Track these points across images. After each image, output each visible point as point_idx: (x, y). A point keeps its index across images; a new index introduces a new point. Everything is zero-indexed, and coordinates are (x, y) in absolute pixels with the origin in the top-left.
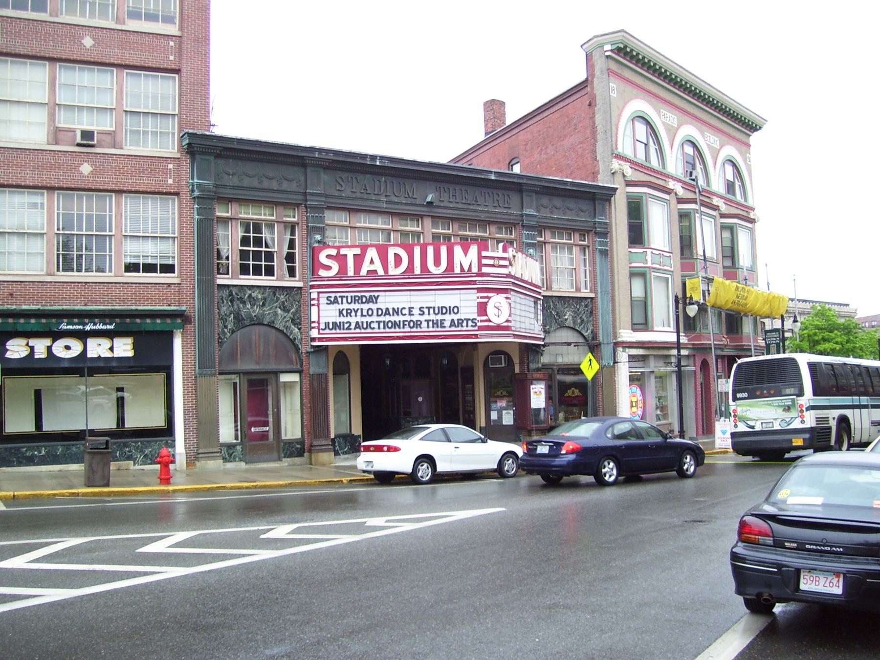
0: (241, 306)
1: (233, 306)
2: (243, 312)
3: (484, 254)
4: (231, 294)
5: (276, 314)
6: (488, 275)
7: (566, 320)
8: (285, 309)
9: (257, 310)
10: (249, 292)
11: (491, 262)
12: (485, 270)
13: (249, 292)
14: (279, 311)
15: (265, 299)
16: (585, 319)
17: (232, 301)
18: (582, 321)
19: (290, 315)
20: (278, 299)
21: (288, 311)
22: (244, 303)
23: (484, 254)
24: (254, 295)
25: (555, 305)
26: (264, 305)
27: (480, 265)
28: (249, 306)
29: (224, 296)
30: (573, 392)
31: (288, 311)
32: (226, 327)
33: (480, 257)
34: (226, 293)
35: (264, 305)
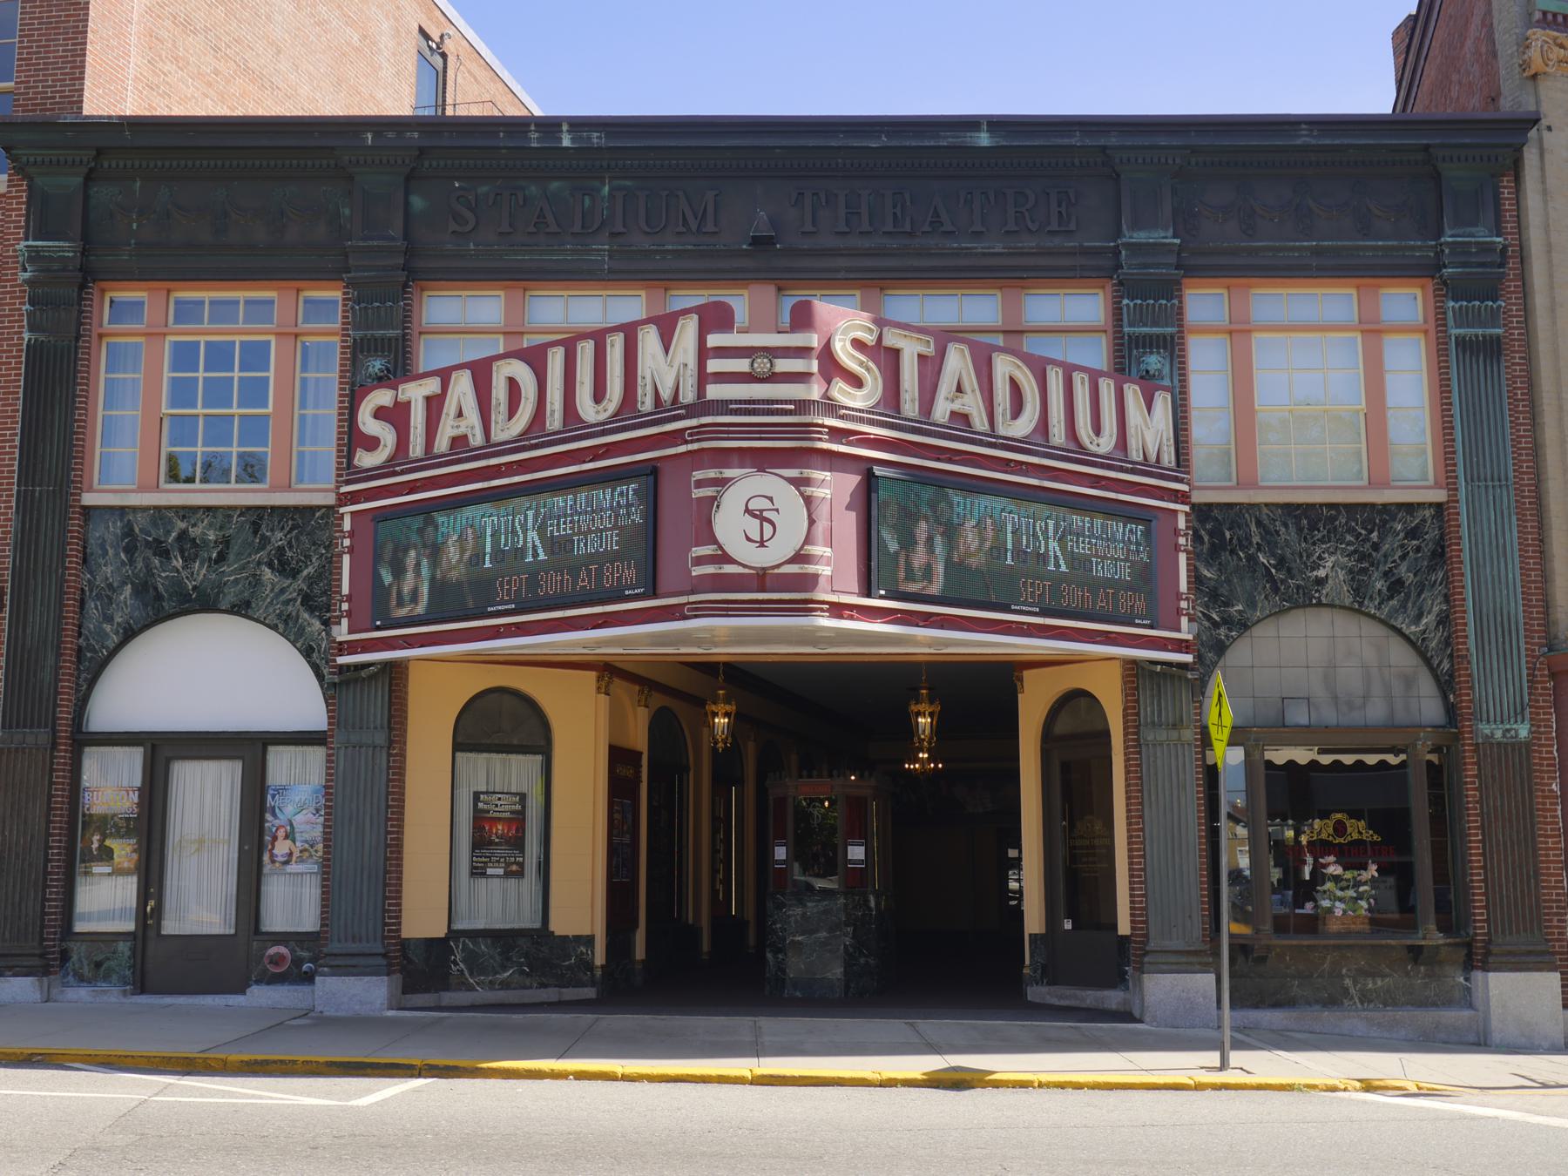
0: (156, 561)
1: (131, 562)
2: (162, 579)
3: (714, 340)
4: (129, 532)
5: (256, 582)
6: (723, 406)
7: (1321, 582)
8: (285, 568)
9: (200, 571)
10: (182, 525)
11: (742, 365)
12: (714, 392)
13: (182, 525)
14: (267, 574)
15: (226, 542)
16: (1409, 578)
17: (130, 550)
18: (1396, 586)
19: (300, 583)
20: (265, 541)
21: (294, 574)
22: (165, 554)
23: (714, 340)
24: (195, 532)
25: (1268, 534)
26: (222, 558)
27: (703, 378)
28: (178, 563)
29: (109, 538)
30: (1340, 829)
31: (294, 574)
32: (109, 619)
33: (703, 353)
34: (115, 527)
35: (222, 558)
